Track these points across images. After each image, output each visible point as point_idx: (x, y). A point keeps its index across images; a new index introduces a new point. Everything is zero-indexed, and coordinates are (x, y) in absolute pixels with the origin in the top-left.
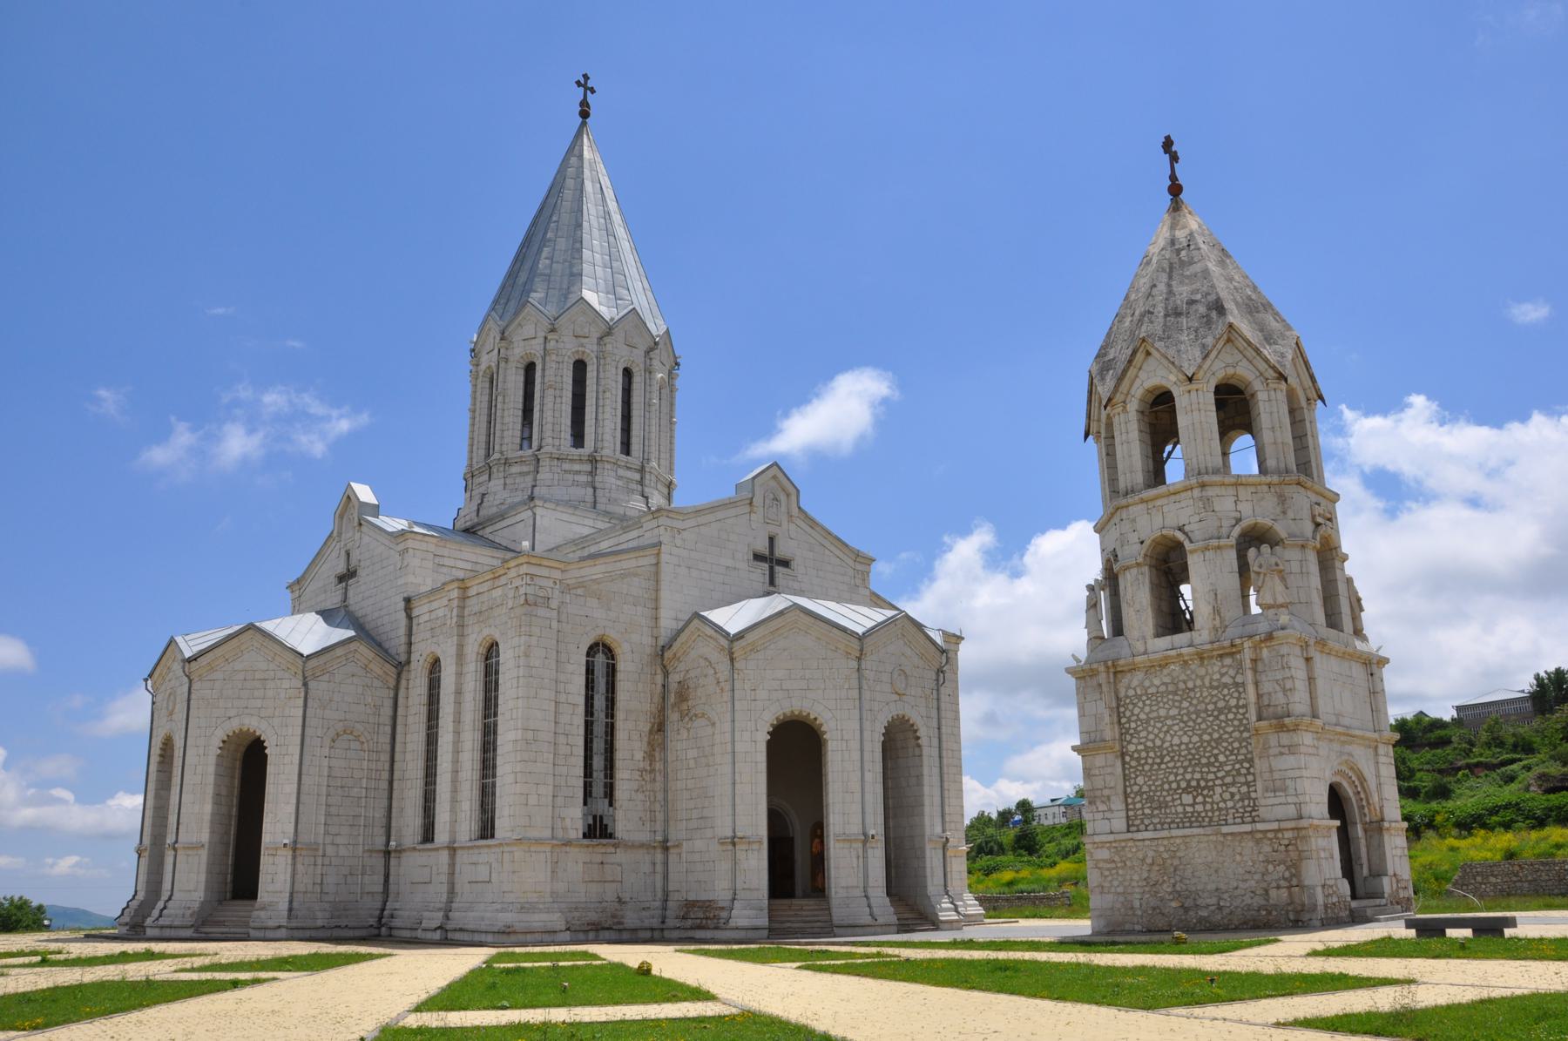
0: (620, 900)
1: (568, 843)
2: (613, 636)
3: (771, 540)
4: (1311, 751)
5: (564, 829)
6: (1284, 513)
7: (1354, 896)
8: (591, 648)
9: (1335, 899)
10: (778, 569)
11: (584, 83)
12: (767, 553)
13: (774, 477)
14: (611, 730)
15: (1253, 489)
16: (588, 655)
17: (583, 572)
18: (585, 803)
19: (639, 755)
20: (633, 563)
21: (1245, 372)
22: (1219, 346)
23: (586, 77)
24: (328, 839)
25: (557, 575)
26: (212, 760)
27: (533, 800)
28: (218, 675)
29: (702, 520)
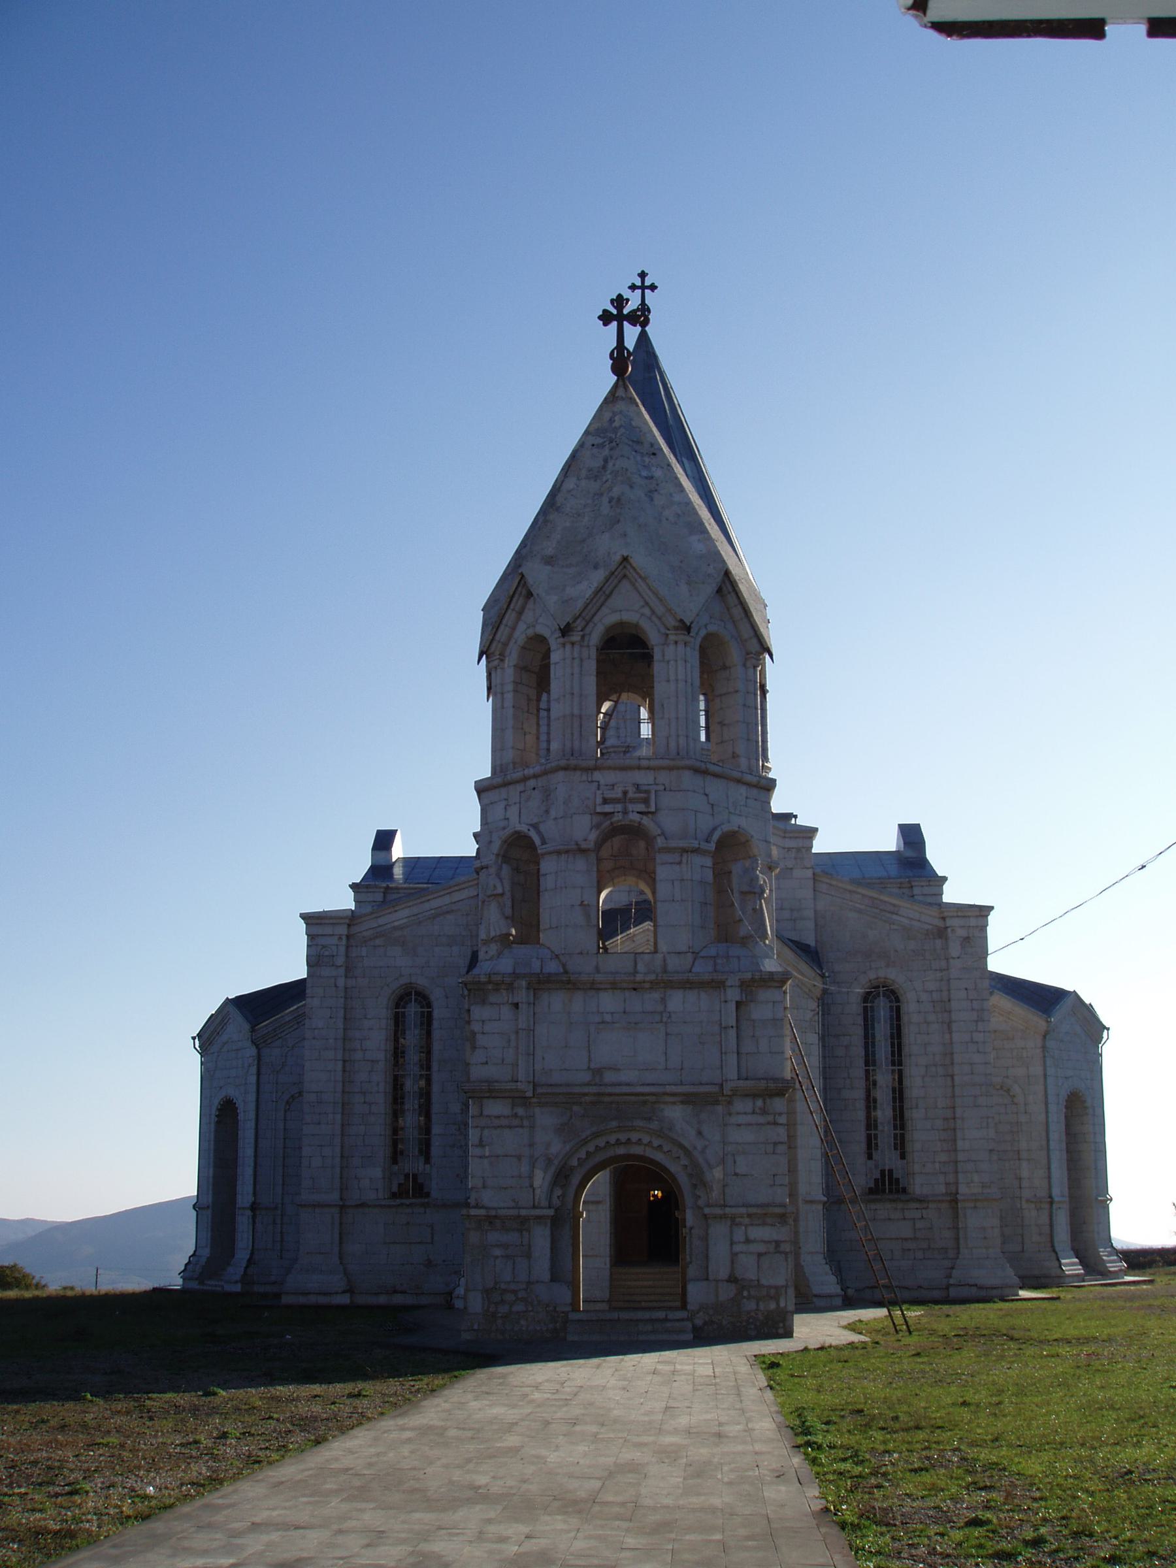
0: (429, 1263)
1: (363, 1205)
2: (422, 982)
6: (547, 812)
8: (401, 998)
9: (520, 1307)
15: (520, 787)
16: (397, 1006)
17: (381, 921)
18: (395, 1160)
20: (447, 900)
21: (547, 628)
22: (518, 603)
23: (643, 275)
25: (343, 930)
26: (213, 1126)
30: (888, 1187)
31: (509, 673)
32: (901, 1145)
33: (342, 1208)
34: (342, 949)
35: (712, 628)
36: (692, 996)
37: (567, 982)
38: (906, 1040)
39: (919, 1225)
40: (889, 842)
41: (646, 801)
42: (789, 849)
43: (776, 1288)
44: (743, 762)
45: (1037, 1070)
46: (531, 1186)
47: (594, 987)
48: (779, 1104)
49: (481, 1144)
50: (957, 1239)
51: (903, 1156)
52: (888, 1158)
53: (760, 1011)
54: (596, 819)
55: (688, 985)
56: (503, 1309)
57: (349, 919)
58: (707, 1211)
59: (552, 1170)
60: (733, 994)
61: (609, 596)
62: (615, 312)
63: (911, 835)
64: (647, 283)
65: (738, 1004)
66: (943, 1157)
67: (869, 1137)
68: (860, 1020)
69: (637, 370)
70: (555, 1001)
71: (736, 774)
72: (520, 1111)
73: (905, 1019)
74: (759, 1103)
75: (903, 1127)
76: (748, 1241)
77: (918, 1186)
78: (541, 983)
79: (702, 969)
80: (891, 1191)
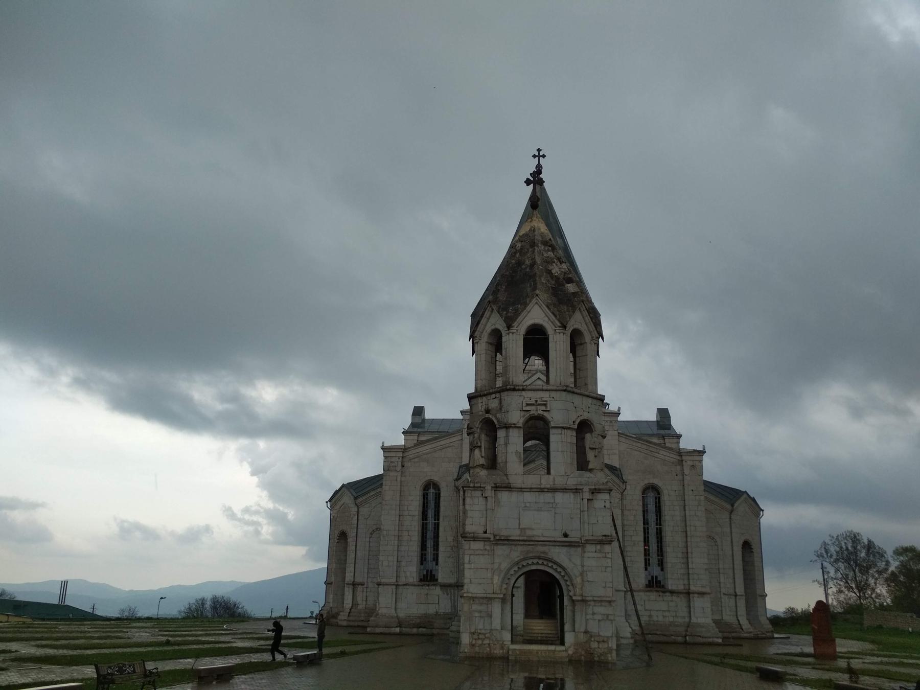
1: (406, 585)
2: (436, 479)
4: (481, 552)
5: (406, 577)
7: (513, 642)
9: (487, 641)
11: (539, 155)
14: (437, 527)
18: (422, 564)
19: (450, 539)
20: (448, 441)
23: (539, 150)
24: (370, 580)
25: (400, 454)
27: (385, 563)
28: (338, 507)
30: (655, 584)
31: (482, 346)
32: (661, 564)
33: (397, 585)
34: (400, 464)
35: (576, 326)
36: (567, 495)
37: (509, 488)
38: (663, 514)
40: (652, 416)
41: (545, 405)
43: (608, 637)
44: (590, 387)
45: (728, 530)
47: (521, 490)
48: (607, 548)
49: (469, 562)
50: (690, 612)
51: (662, 570)
52: (655, 570)
54: (523, 413)
55: (564, 490)
56: (480, 642)
57: (404, 449)
58: (574, 598)
59: (502, 575)
60: (587, 495)
63: (664, 414)
66: (682, 571)
67: (645, 559)
69: (538, 203)
70: (504, 496)
71: (587, 393)
72: (488, 548)
73: (662, 503)
74: (599, 547)
75: (662, 555)
76: (594, 614)
77: (671, 585)
78: (497, 488)
79: (571, 482)
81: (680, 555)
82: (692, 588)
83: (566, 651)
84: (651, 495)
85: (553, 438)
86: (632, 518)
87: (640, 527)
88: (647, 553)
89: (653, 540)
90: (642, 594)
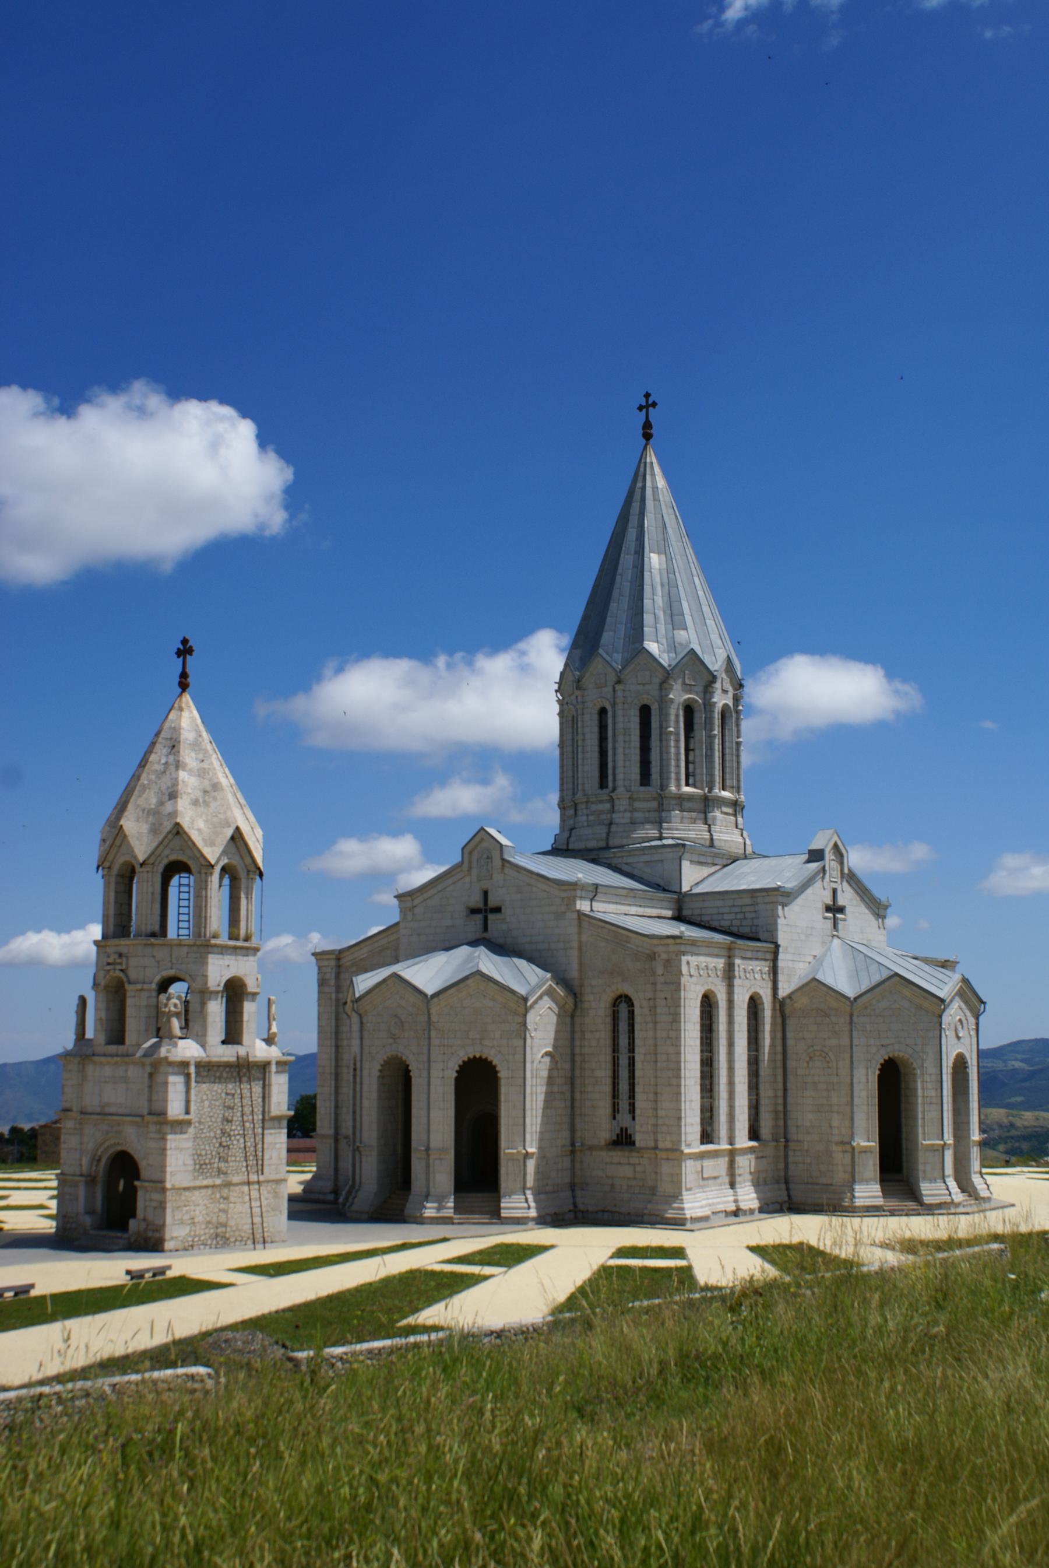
3: (486, 894)
9: (73, 1226)
10: (491, 917)
11: (648, 405)
12: (481, 905)
13: (482, 840)
20: (385, 941)
23: (647, 395)
29: (426, 895)
39: (638, 1168)
42: (563, 898)
45: (846, 1041)
46: (81, 1165)
53: (159, 1079)
61: (120, 846)
62: (181, 647)
64: (650, 402)
65: (151, 1075)
66: (652, 1121)
68: (609, 1020)
70: (90, 1069)
77: (639, 1139)
80: (626, 1144)
81: (651, 1097)
82: (661, 1145)
83: (129, 1238)
84: (623, 1008)
85: (129, 1002)
86: (594, 1043)
87: (606, 1057)
88: (615, 1095)
89: (624, 1073)
90: (604, 1154)
